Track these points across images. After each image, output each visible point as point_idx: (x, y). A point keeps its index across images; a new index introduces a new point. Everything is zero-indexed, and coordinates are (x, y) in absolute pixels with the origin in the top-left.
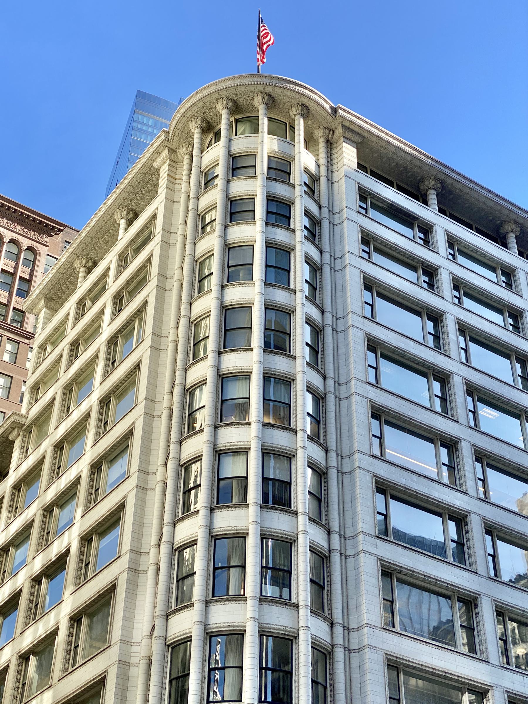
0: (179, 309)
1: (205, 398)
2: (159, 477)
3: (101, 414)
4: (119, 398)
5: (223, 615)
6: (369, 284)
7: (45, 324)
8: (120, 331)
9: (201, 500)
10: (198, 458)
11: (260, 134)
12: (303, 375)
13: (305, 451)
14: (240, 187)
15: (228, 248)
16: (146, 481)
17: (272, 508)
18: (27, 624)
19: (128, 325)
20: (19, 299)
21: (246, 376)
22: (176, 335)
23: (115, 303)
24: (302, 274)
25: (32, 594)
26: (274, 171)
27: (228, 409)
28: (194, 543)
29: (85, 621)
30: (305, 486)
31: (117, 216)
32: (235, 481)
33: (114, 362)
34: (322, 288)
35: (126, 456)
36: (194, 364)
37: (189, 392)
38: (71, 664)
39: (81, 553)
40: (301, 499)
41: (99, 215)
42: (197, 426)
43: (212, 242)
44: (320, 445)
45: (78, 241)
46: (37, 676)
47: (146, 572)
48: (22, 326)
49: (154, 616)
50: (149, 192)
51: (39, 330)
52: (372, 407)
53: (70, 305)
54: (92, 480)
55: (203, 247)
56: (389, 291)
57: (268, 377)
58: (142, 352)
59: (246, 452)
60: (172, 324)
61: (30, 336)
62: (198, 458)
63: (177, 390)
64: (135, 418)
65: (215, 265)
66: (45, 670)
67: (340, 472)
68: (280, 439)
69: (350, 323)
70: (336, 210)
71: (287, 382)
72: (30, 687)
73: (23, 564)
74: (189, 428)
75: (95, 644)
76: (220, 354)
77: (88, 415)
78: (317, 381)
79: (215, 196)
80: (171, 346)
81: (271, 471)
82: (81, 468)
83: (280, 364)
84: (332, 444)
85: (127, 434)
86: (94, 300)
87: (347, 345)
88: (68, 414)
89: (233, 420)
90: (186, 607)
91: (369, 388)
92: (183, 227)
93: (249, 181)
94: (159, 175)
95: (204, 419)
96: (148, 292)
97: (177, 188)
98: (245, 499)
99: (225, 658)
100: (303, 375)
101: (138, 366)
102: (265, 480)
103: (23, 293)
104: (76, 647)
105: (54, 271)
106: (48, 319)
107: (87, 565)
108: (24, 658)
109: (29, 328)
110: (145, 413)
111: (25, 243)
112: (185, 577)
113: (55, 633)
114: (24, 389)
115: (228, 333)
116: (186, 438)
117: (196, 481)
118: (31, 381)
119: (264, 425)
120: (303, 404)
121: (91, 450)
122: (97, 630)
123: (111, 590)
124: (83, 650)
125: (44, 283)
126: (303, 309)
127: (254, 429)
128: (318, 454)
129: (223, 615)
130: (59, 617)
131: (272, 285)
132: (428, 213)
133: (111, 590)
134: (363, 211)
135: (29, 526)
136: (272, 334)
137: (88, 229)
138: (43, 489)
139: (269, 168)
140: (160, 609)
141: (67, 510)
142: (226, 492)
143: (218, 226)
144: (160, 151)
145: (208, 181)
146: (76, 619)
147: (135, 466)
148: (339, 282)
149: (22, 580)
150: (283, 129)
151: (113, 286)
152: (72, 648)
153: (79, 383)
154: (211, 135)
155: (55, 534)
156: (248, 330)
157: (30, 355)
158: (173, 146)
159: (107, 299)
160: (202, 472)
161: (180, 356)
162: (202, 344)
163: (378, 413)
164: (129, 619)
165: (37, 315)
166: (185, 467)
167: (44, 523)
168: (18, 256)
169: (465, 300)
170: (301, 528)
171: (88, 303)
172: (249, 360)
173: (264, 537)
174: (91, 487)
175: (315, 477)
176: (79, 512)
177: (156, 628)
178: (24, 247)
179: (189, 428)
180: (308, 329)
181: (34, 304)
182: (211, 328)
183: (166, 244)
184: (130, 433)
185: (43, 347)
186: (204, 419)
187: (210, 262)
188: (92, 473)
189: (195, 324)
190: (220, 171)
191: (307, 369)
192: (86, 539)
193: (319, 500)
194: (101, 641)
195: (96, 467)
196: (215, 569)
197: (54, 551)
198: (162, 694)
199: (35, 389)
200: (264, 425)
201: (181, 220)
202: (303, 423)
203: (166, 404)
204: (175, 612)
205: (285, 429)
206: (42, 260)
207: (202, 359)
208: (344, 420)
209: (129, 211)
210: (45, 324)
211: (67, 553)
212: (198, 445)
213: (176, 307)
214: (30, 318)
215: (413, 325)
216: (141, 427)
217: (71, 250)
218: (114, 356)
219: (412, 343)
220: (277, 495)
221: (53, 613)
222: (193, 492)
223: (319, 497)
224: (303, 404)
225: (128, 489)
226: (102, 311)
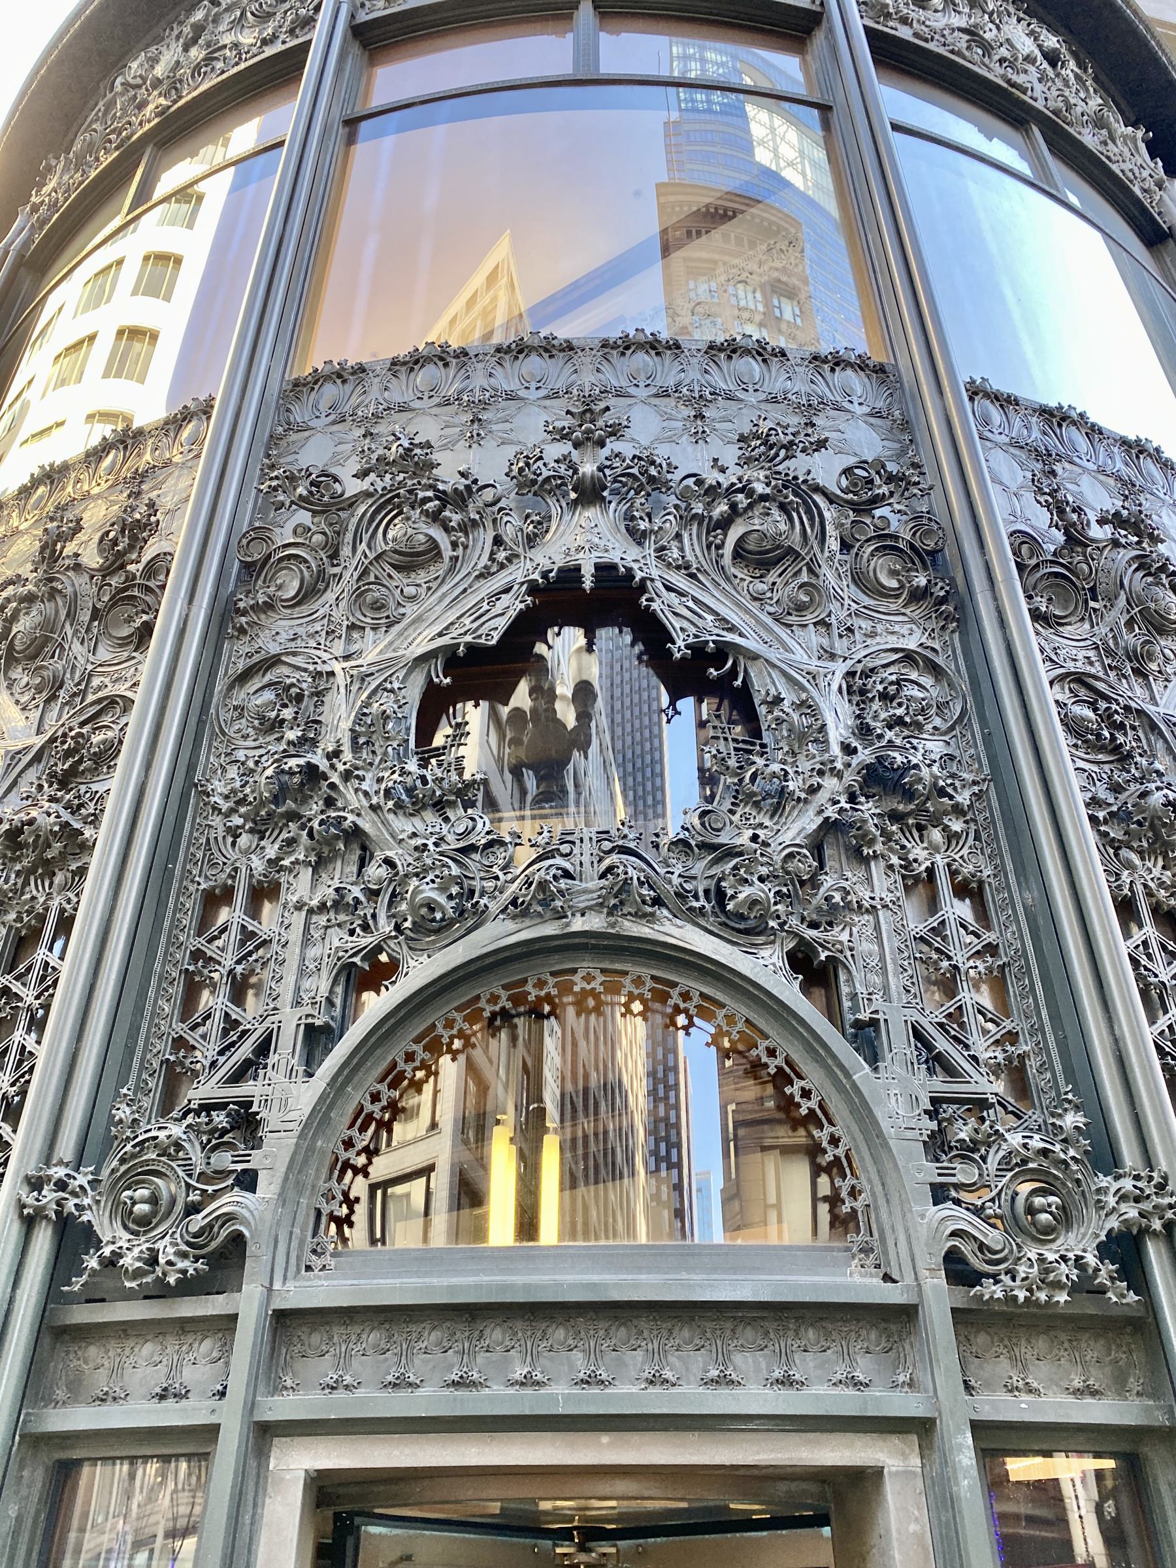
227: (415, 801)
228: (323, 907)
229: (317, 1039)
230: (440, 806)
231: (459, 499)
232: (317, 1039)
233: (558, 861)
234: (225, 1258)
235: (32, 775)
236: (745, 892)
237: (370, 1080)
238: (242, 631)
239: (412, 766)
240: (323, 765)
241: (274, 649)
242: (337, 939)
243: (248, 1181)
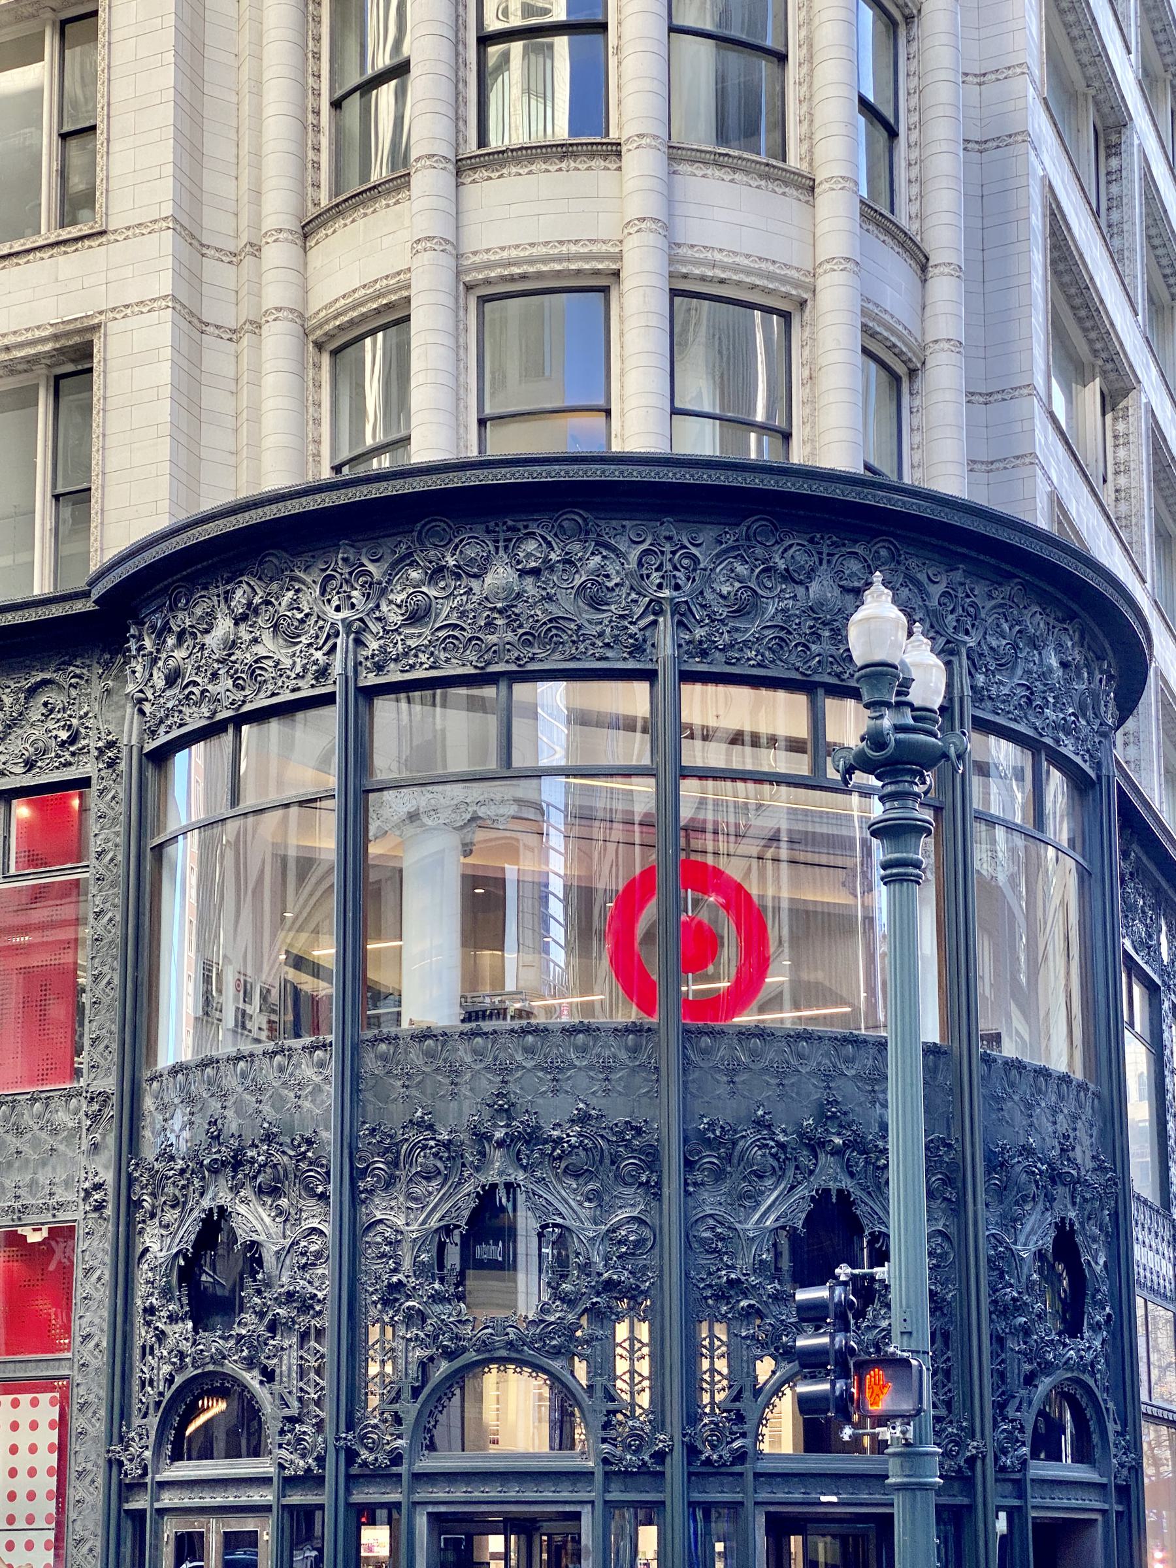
227: (437, 1298)
228: (410, 1340)
229: (416, 1392)
230: (449, 1301)
231: (447, 1145)
232: (416, 1392)
233: (489, 1331)
234: (397, 1459)
235: (287, 1262)
236: (554, 1342)
237: (433, 1402)
238: (364, 1202)
239: (437, 1286)
240: (404, 1280)
241: (379, 1217)
242: (418, 1353)
243: (400, 1437)
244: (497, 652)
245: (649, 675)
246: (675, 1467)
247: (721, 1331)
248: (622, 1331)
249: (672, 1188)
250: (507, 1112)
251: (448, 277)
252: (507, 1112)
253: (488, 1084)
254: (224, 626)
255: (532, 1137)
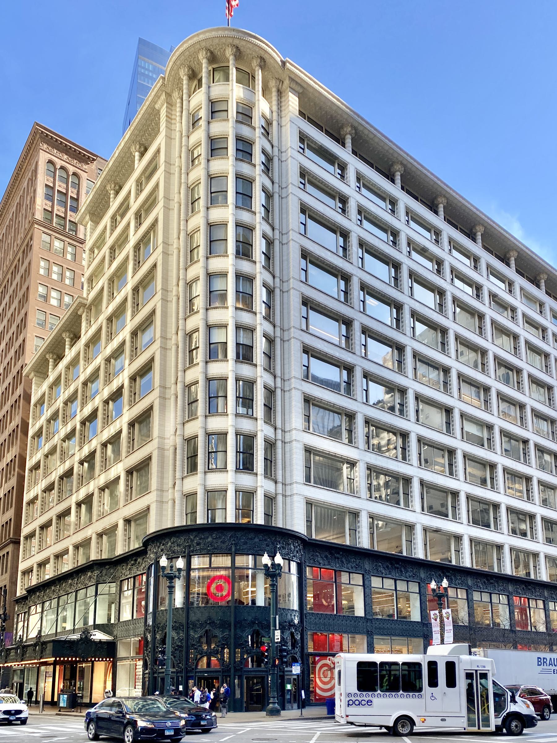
0: (180, 224)
1: (199, 289)
2: (173, 341)
3: (134, 299)
4: (145, 288)
5: (216, 424)
6: (304, 209)
7: (92, 233)
8: (141, 239)
9: (200, 356)
10: (197, 330)
11: (230, 83)
12: (261, 276)
13: (262, 327)
14: (217, 128)
15: (211, 178)
16: (166, 344)
17: (242, 362)
18: (104, 427)
19: (146, 235)
20: (72, 214)
21: (224, 275)
22: (178, 244)
23: (136, 218)
24: (260, 200)
25: (105, 410)
26: (240, 115)
27: (214, 297)
28: (197, 382)
29: (137, 426)
30: (261, 349)
31: (133, 149)
32: (219, 345)
33: (139, 262)
34: (273, 211)
35: (152, 327)
36: (191, 265)
37: (189, 285)
38: (131, 450)
39: (131, 387)
40: (259, 357)
41: (120, 148)
42: (195, 308)
43: (198, 173)
44: (271, 322)
45: (107, 169)
46: (112, 456)
47: (170, 399)
48: (76, 234)
49: (176, 424)
50: (153, 129)
51: (88, 237)
52: (303, 297)
53: (106, 220)
54: (132, 342)
55: (193, 176)
56: (317, 214)
57: (239, 276)
58: (157, 256)
59: (226, 326)
60: (175, 236)
61: (82, 242)
62: (197, 330)
63: (181, 283)
64: (156, 302)
65: (202, 192)
66: (117, 452)
67: (282, 340)
68: (246, 318)
69: (291, 238)
70: (283, 150)
71: (250, 279)
72: (109, 461)
73: (97, 392)
74: (191, 311)
75: (144, 438)
76: (207, 258)
77: (126, 299)
78: (269, 279)
79: (199, 135)
80: (176, 252)
81: (241, 339)
82: (125, 334)
83: (245, 267)
84: (278, 323)
85: (152, 313)
86: (123, 216)
87: (288, 254)
88: (113, 298)
89: (217, 305)
90: (194, 419)
91: (301, 284)
92: (179, 160)
93: (224, 123)
94: (160, 115)
95: (199, 303)
96: (158, 211)
97: (173, 127)
98: (226, 356)
99: (217, 447)
100: (261, 276)
101: (155, 266)
102: (238, 344)
103: (75, 209)
104: (133, 440)
105: (93, 193)
106: (93, 230)
107: (135, 394)
108: (104, 445)
109: (81, 236)
110: (162, 299)
111: (71, 169)
112: (193, 402)
113: (120, 432)
114: (83, 280)
115: (212, 243)
116: (189, 316)
117: (196, 344)
118: (87, 274)
119: (237, 308)
120: (260, 295)
121: (130, 323)
122: (144, 431)
123: (150, 409)
124: (138, 441)
125: (88, 202)
126: (261, 227)
127: (231, 311)
128: (269, 328)
129: (216, 424)
130: (122, 423)
131: (240, 208)
132: (344, 154)
133: (150, 409)
134: (301, 151)
135: (98, 370)
136: (241, 244)
137: (113, 159)
138: (103, 347)
139: (237, 112)
140: (179, 420)
141: (119, 360)
142: (214, 352)
143: (203, 159)
144: (159, 95)
145: (195, 123)
146: (131, 425)
147: (158, 335)
148: (284, 206)
149: (98, 401)
150: (246, 78)
151: (134, 206)
152: (131, 440)
153: (118, 276)
154: (196, 82)
155: (114, 375)
156: (225, 242)
157: (84, 256)
158: (169, 91)
159: (130, 215)
160: (200, 339)
161: (182, 259)
162: (196, 251)
163: (306, 302)
164: (162, 425)
165: (85, 226)
166: (189, 336)
167: (106, 368)
168: (67, 179)
169: (365, 222)
170: (259, 374)
171: (119, 218)
172: (227, 263)
173: (237, 380)
174: (132, 347)
175: (268, 344)
176: (127, 362)
177: (178, 430)
178: (71, 173)
179: (191, 311)
180: (264, 241)
181: (83, 218)
182: (201, 239)
183: (168, 173)
184: (153, 312)
185: (92, 250)
186: (199, 303)
187: (198, 188)
188: (132, 338)
189: (190, 236)
190: (203, 114)
191: (263, 271)
192: (133, 379)
193: (270, 358)
194: (147, 436)
195: (134, 334)
196: (209, 398)
197: (114, 386)
198: (183, 465)
199: (90, 280)
200: (237, 308)
201: (177, 154)
202: (260, 307)
203: (174, 293)
204: (188, 421)
205: (250, 311)
206: (84, 184)
207: (196, 262)
208: (285, 306)
209: (141, 145)
210: (92, 233)
211: (122, 387)
212: (196, 321)
213: (178, 224)
214: (81, 228)
215: (331, 240)
216: (160, 308)
217: (103, 176)
218: (139, 258)
219: (329, 253)
220: (245, 354)
221: (118, 421)
222: (194, 351)
223: (269, 356)
224: (260, 295)
225: (155, 348)
226: (128, 224)
244: (210, 550)
245: (231, 554)
246: (232, 671)
247: (239, 650)
248: (226, 650)
249: (232, 630)
250: (210, 619)
251: (203, 490)
252: (210, 619)
253: (207, 615)
254: (170, 544)
255: (213, 622)
